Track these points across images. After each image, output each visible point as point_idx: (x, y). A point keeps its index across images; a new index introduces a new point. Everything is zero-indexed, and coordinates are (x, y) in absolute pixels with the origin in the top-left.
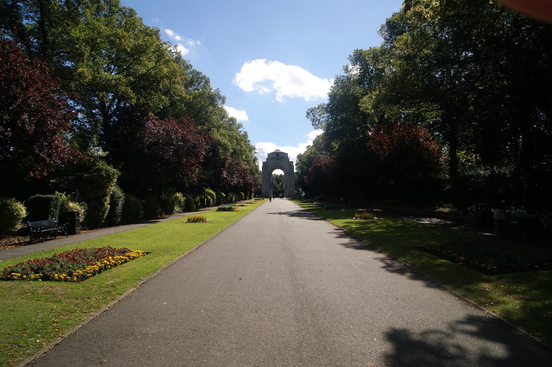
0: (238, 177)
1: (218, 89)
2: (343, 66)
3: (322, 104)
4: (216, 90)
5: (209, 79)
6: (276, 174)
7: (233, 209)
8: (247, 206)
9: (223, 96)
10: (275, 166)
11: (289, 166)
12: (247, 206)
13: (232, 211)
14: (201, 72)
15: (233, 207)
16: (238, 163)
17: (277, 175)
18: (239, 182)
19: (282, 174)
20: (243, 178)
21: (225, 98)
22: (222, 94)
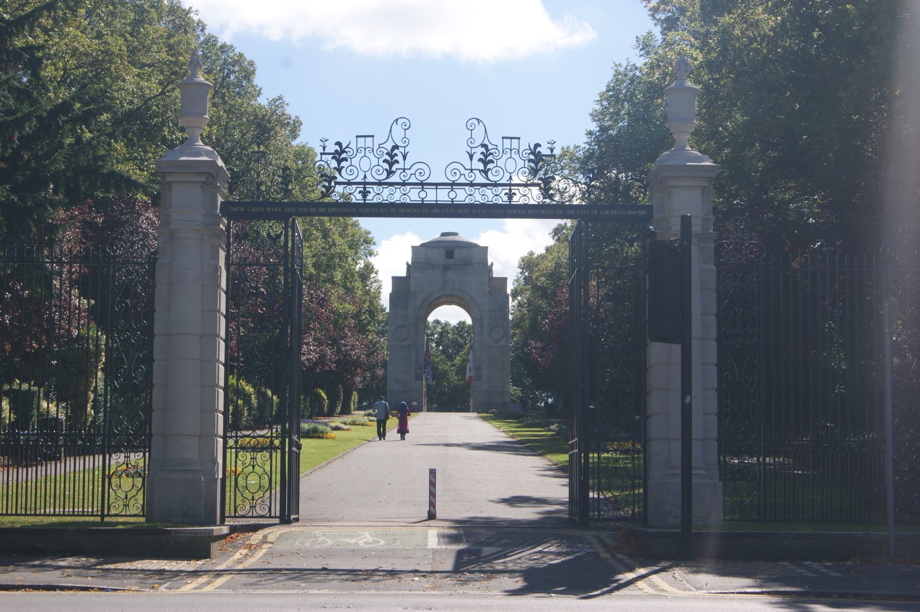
0: (319, 342)
1: (280, 98)
2: (637, 37)
3: (572, 148)
4: (275, 100)
5: (252, 64)
6: (443, 321)
7: (323, 433)
8: (348, 430)
9: (293, 117)
10: (437, 295)
11: (490, 292)
12: (348, 430)
13: (319, 437)
14: (232, 46)
15: (320, 427)
16: (323, 299)
17: (447, 324)
18: (323, 356)
19: (464, 323)
20: (335, 342)
21: (301, 124)
22: (291, 111)
